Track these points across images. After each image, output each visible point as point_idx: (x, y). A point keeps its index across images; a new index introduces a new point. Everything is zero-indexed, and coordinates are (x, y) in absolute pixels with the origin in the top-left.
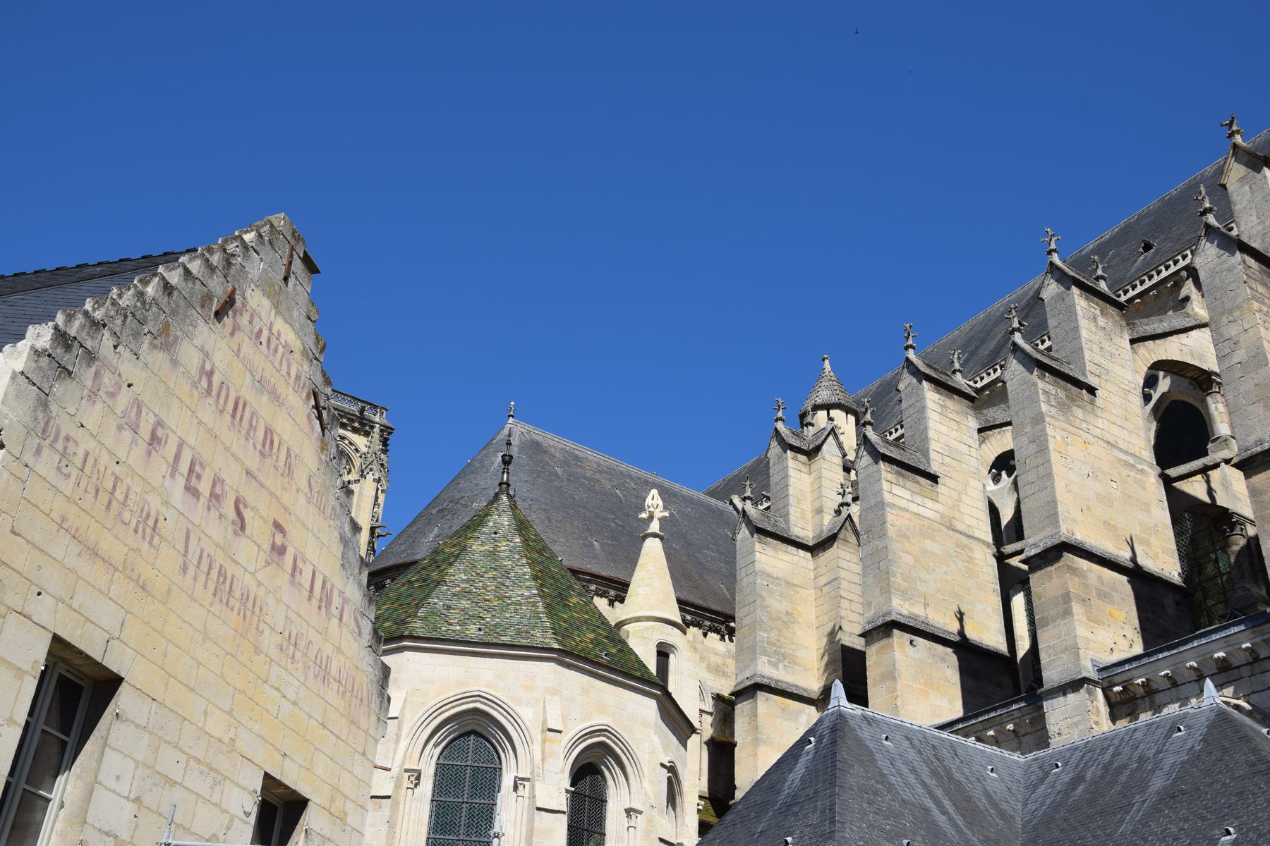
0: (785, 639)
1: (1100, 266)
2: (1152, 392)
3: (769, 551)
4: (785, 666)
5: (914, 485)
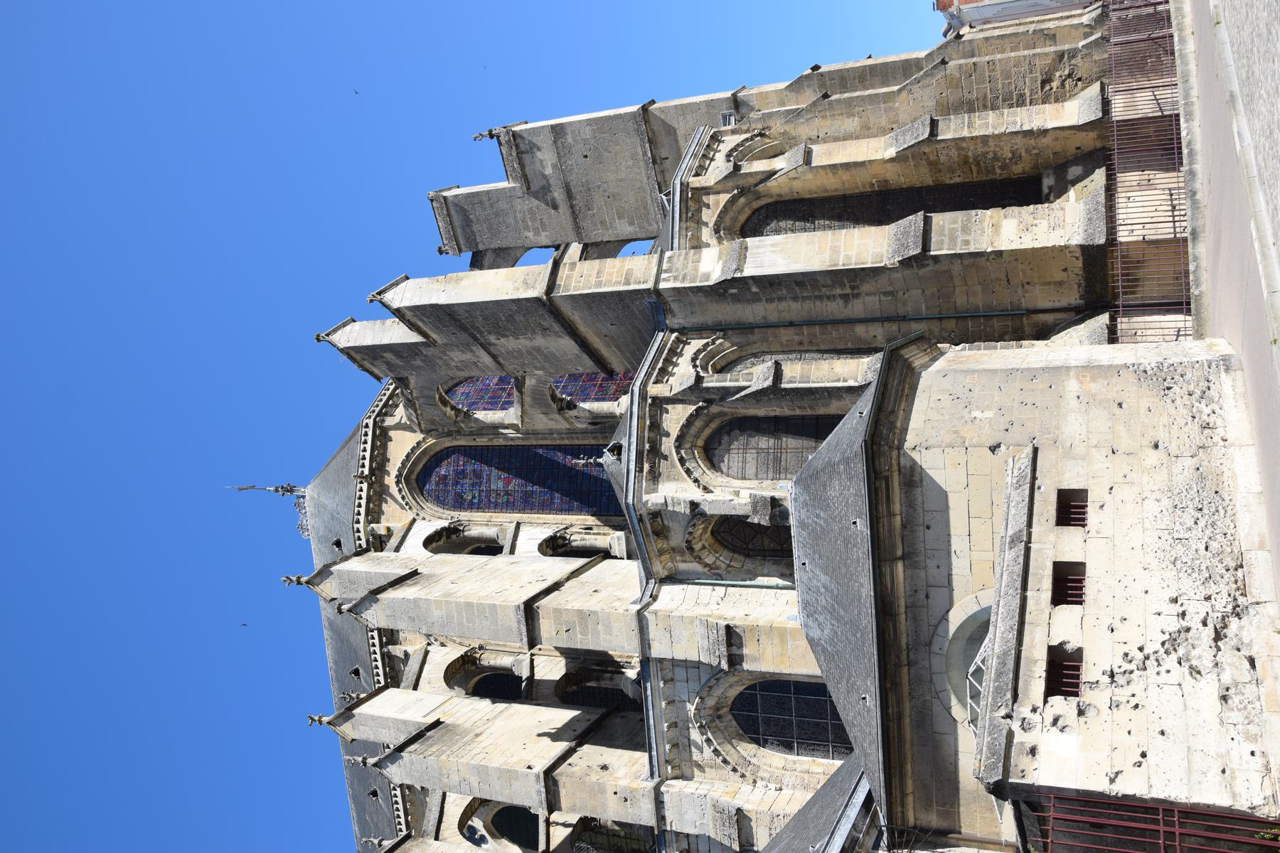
1: (372, 839)
2: (479, 833)
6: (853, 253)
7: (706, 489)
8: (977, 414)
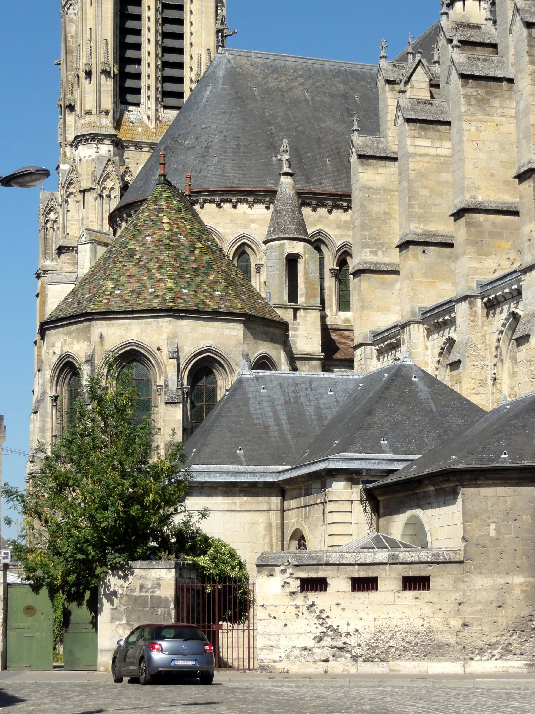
0: (384, 232)
3: (370, 170)
4: (383, 251)
5: (434, 133)
8: (493, 526)
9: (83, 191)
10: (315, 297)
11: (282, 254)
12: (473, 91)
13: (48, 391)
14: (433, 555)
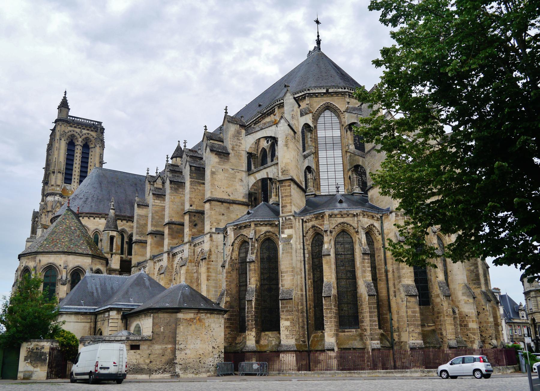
3: (141, 209)
6: (285, 278)
7: (232, 245)
8: (162, 328)
9: (48, 212)
10: (119, 250)
11: (108, 235)
12: (173, 186)
13: (19, 279)
14: (142, 338)
